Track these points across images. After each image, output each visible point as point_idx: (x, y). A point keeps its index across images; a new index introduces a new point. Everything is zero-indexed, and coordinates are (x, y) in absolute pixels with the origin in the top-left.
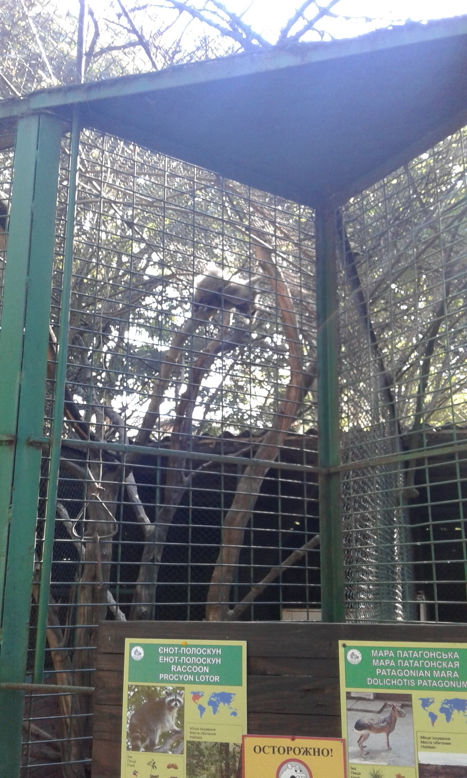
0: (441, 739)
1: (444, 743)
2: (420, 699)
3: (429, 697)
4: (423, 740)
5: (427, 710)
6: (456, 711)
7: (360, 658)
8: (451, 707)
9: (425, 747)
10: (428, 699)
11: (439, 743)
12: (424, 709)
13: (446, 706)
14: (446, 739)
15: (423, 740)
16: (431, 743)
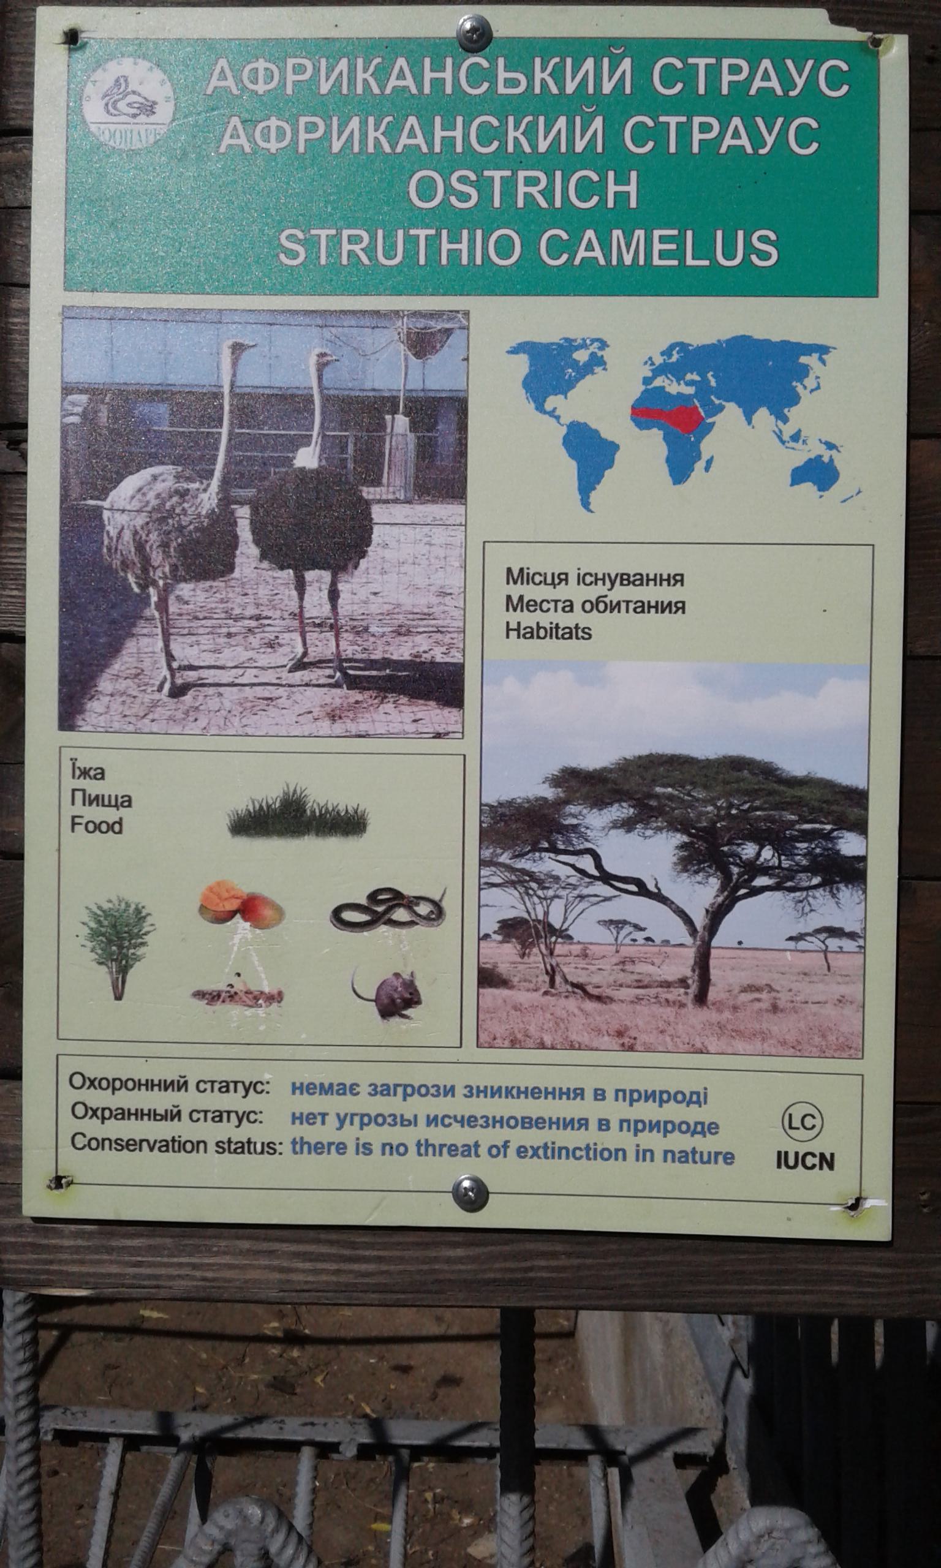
0: (625, 579)
1: (643, 607)
2: (515, 351)
3: (576, 333)
4: (516, 591)
5: (552, 414)
6: (732, 412)
8: (702, 388)
9: (532, 633)
10: (569, 346)
11: (615, 607)
12: (540, 408)
13: (674, 388)
14: (658, 580)
15: (516, 591)
16: (569, 607)
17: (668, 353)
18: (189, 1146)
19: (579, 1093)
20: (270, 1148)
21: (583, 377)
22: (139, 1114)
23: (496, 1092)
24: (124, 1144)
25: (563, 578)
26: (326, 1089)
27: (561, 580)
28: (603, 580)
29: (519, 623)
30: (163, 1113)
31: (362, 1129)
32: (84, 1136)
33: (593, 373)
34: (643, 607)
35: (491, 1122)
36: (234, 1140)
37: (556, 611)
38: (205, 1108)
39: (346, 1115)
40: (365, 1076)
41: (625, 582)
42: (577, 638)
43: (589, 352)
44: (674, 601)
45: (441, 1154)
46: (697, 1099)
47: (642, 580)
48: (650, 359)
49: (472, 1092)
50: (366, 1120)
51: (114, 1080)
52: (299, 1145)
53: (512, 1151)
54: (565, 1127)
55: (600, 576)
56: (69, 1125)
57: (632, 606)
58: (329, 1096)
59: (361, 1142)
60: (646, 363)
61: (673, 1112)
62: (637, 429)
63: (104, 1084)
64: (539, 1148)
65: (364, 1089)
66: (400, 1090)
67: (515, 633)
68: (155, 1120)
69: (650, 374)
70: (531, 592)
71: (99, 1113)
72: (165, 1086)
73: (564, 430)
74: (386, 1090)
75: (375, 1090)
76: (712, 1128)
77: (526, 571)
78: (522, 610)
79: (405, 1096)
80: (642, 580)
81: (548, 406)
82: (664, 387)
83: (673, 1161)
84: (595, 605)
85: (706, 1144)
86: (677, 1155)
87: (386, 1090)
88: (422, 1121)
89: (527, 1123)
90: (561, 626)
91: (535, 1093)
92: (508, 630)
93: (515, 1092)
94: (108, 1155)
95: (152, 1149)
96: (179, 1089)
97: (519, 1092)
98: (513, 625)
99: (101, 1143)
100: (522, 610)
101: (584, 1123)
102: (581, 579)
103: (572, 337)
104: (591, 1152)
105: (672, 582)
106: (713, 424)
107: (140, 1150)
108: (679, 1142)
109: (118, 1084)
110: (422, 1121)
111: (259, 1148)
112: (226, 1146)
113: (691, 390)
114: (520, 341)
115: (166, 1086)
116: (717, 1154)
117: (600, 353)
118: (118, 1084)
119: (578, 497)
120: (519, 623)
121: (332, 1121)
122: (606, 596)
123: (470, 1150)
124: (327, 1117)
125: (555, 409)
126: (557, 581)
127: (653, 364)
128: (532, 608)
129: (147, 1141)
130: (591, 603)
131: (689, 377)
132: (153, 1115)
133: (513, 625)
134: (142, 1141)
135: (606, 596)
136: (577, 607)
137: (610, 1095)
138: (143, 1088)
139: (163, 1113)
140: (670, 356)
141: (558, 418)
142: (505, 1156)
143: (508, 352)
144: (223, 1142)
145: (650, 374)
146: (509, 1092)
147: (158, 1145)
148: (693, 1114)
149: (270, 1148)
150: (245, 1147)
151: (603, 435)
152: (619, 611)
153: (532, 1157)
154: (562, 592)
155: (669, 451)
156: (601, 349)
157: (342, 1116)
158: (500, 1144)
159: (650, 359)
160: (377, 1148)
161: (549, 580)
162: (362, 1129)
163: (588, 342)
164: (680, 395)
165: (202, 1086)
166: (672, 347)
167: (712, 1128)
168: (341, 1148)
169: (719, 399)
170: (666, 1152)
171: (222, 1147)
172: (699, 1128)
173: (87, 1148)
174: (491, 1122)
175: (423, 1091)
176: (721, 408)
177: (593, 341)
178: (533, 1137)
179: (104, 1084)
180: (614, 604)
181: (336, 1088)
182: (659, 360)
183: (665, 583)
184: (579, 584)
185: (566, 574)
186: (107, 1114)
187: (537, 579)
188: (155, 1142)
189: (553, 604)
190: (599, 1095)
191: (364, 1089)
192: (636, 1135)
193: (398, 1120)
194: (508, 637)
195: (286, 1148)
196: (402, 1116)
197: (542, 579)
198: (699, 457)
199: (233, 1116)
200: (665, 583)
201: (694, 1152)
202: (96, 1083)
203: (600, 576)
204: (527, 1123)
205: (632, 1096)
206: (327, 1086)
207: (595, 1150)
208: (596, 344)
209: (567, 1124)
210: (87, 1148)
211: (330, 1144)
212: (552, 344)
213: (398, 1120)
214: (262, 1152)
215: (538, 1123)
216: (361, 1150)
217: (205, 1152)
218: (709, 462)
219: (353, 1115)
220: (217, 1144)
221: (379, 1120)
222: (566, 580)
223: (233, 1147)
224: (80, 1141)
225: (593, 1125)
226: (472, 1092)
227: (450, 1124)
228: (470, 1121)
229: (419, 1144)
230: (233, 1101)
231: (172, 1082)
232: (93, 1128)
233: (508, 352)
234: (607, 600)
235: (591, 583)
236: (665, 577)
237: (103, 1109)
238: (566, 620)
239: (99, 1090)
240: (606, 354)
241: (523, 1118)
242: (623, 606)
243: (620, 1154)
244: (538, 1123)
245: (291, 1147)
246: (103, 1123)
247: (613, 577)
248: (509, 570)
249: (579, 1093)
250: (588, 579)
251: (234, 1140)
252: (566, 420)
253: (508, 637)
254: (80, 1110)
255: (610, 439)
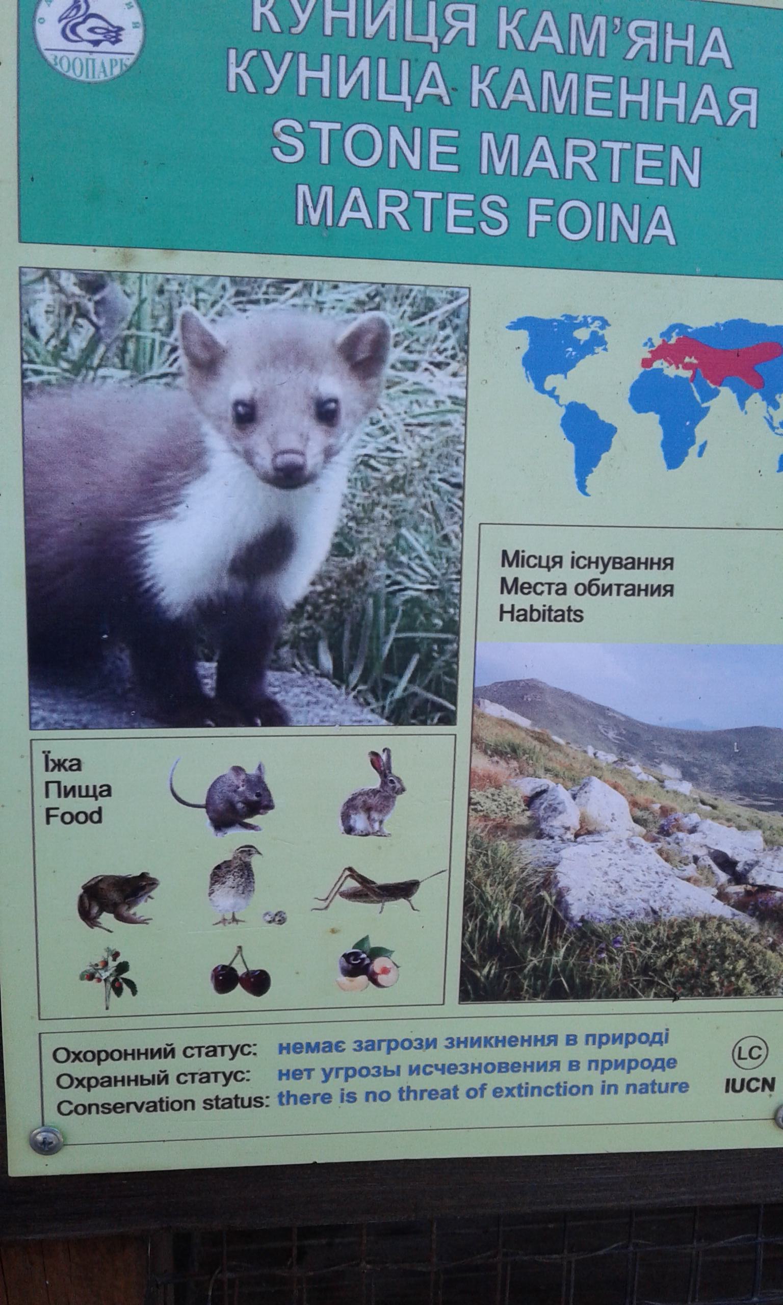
0: (618, 563)
1: (634, 590)
3: (580, 312)
4: (510, 573)
5: (552, 394)
7: (132, 41)
9: (525, 616)
10: (570, 323)
11: (606, 590)
12: (540, 388)
13: (671, 371)
14: (649, 563)
15: (510, 573)
16: (562, 590)
17: (666, 334)
18: (176, 1106)
19: (553, 1040)
20: (258, 1102)
21: (582, 357)
22: (126, 1081)
23: (475, 1042)
24: (111, 1107)
25: (558, 561)
26: (312, 1048)
27: (555, 563)
28: (597, 563)
29: (513, 606)
30: (150, 1078)
31: (346, 1080)
32: (70, 1103)
33: (593, 353)
34: (634, 590)
35: (468, 1068)
36: (222, 1097)
37: (549, 593)
38: (193, 1071)
39: (331, 1069)
40: (350, 1034)
41: (617, 566)
42: (569, 620)
43: (590, 330)
44: (663, 585)
45: (422, 1098)
46: (660, 1038)
47: (634, 563)
48: (650, 340)
49: (454, 1043)
50: (350, 1073)
51: (99, 1052)
52: (285, 1098)
53: (488, 1092)
54: (539, 1069)
55: (594, 559)
56: (54, 1095)
57: (623, 589)
58: (315, 1054)
59: (346, 1092)
60: (645, 344)
61: (638, 1051)
62: (634, 412)
63: (89, 1056)
64: (513, 1088)
65: (349, 1046)
66: (384, 1045)
67: (509, 615)
68: (142, 1084)
69: (649, 356)
70: (526, 575)
71: (85, 1082)
72: (152, 1054)
73: (563, 411)
74: (372, 1045)
75: (360, 1046)
76: (672, 1063)
77: (521, 554)
78: (516, 593)
79: (389, 1049)
80: (634, 563)
81: (548, 386)
82: (662, 370)
83: (635, 1092)
84: (587, 589)
85: (663, 1077)
86: (638, 1088)
87: (372, 1045)
88: (404, 1071)
89: (503, 1067)
90: (554, 608)
91: (512, 1041)
92: (502, 612)
93: (493, 1041)
94: (94, 1117)
95: (139, 1109)
96: (166, 1057)
97: (497, 1041)
98: (507, 608)
99: (87, 1109)
100: (516, 593)
101: (556, 1065)
102: (575, 562)
103: (575, 315)
104: (561, 1089)
105: (663, 565)
106: (708, 409)
107: (128, 1111)
108: (641, 1076)
109: (103, 1056)
110: (404, 1071)
111: (246, 1103)
112: (214, 1103)
113: (688, 374)
114: (521, 316)
115: (152, 1054)
116: (674, 1084)
117: (601, 333)
118: (103, 1056)
119: (574, 480)
120: (513, 606)
121: (318, 1075)
122: (598, 579)
123: (450, 1094)
124: (313, 1073)
125: (554, 389)
126: (551, 564)
127: (652, 345)
128: (526, 591)
129: (135, 1103)
130: (583, 585)
131: (687, 360)
132: (140, 1080)
133: (507, 608)
134: (129, 1104)
135: (598, 579)
136: (570, 590)
137: (581, 1040)
138: (130, 1057)
139: (150, 1078)
140: (670, 337)
141: (557, 398)
142: (482, 1096)
143: (509, 328)
144: (211, 1100)
145: (649, 356)
146: (487, 1041)
147: (145, 1106)
148: (654, 1052)
149: (258, 1102)
150: (234, 1102)
151: (602, 417)
152: (611, 594)
153: (507, 1096)
154: (556, 575)
155: (665, 435)
156: (602, 328)
157: (328, 1071)
158: (478, 1087)
159: (650, 340)
160: (361, 1097)
161: (544, 563)
162: (346, 1080)
163: (589, 320)
164: (676, 376)
165: (189, 1052)
166: (672, 328)
167: (672, 1063)
168: (326, 1098)
169: (715, 383)
170: (628, 1086)
171: (209, 1104)
172: (659, 1064)
173: (74, 1114)
174: (468, 1068)
175: (405, 1044)
176: (716, 394)
177: (595, 319)
178: (509, 1079)
179: (89, 1056)
180: (606, 587)
181: (322, 1046)
182: (658, 342)
183: (655, 567)
184: (572, 567)
185: (561, 557)
186: (93, 1082)
187: (533, 561)
188: (143, 1103)
189: (547, 586)
190: (571, 1040)
191: (349, 1046)
192: (602, 1073)
193: (382, 1071)
194: (501, 619)
195: (273, 1101)
196: (385, 1067)
197: (537, 561)
198: (693, 442)
199: (220, 1076)
200: (655, 567)
201: (654, 1083)
202: (81, 1056)
203: (594, 559)
204: (503, 1067)
205: (600, 1040)
206: (313, 1045)
207: (565, 1087)
208: (597, 323)
209: (542, 1067)
210: (74, 1114)
211: (315, 1095)
212: (555, 320)
213: (382, 1071)
214: (249, 1106)
215: (515, 1067)
216: (345, 1098)
217: (193, 1108)
218: (703, 447)
219: (338, 1069)
220: (205, 1102)
221: (363, 1072)
222: (561, 563)
223: (220, 1103)
224: (66, 1108)
225: (564, 1066)
226: (454, 1043)
227: (431, 1073)
228: (451, 1069)
229: (401, 1091)
230: (222, 1063)
231: (159, 1050)
232: (80, 1096)
233: (509, 328)
234: (599, 583)
235: (585, 566)
236: (656, 560)
237: (89, 1079)
238: (559, 603)
239: (85, 1063)
240: (607, 333)
241: (500, 1064)
242: (615, 588)
243: (588, 1089)
244: (515, 1067)
245: (277, 1099)
246: (89, 1090)
247: (606, 560)
248: (505, 553)
249: (553, 1040)
250: (582, 562)
251: (222, 1097)
252: (565, 400)
253: (501, 619)
254: (65, 1081)
255: (608, 420)
